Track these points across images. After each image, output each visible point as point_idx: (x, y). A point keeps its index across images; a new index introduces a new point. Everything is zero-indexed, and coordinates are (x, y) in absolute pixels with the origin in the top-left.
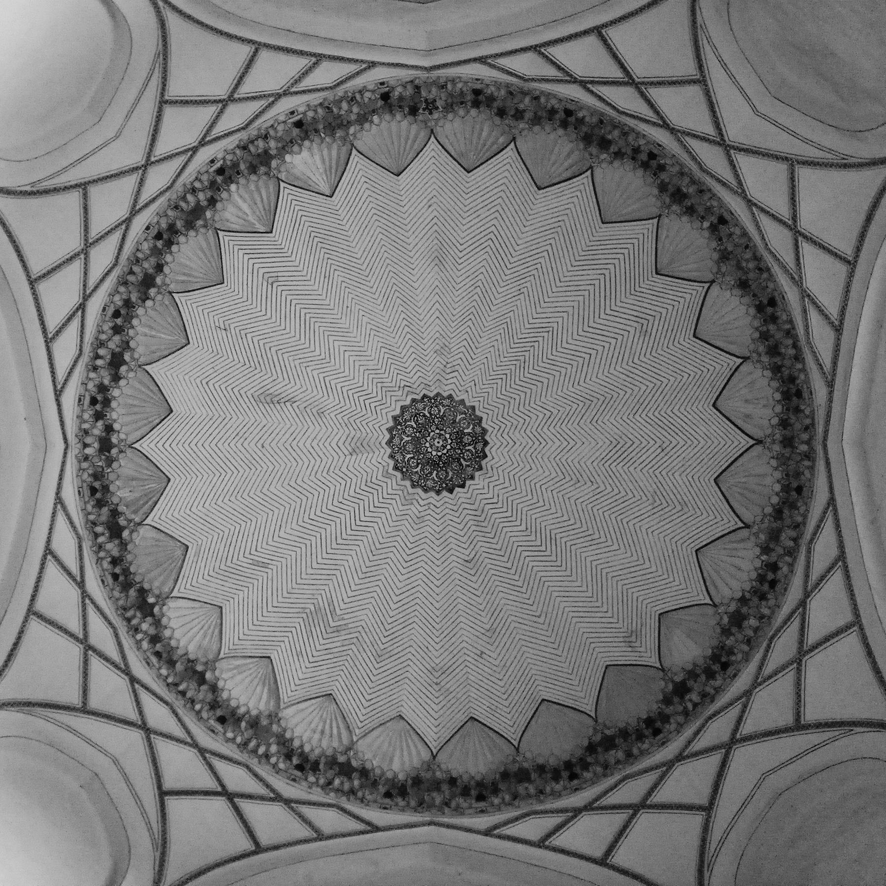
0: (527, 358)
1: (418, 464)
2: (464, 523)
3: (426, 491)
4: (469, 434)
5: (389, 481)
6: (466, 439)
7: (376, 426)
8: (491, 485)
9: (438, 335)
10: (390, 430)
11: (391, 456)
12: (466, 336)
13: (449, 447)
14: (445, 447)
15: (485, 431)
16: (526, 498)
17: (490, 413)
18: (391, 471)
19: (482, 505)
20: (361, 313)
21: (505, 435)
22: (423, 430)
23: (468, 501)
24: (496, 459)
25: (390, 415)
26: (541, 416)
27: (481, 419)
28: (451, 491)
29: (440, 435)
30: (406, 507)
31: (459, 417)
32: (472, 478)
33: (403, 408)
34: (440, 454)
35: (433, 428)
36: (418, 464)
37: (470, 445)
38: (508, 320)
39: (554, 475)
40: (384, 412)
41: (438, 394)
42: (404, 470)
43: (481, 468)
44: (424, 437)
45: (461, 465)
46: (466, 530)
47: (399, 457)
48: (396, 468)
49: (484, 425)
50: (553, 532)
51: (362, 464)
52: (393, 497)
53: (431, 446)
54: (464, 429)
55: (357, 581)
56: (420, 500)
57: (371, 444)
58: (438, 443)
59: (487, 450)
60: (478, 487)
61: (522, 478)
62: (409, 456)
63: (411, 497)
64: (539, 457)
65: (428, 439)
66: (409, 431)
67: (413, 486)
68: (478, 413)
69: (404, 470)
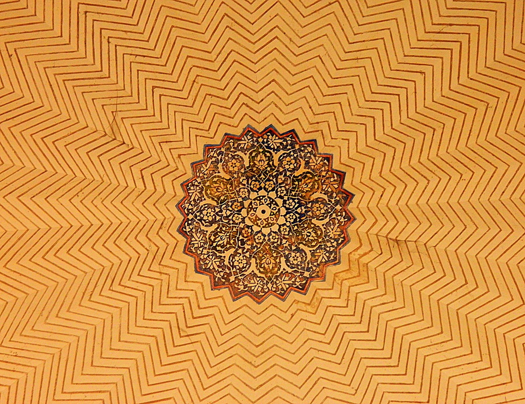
0: (129, 51)
1: (298, 250)
2: (406, 178)
3: (346, 240)
4: (252, 159)
5: (326, 302)
6: (262, 164)
7: (228, 318)
8: (342, 126)
9: (76, 201)
10: (236, 295)
11: (282, 295)
12: (82, 152)
13: (273, 195)
14: (272, 201)
15: (249, 131)
16: (369, 68)
17: (218, 119)
18: (306, 298)
19: (376, 145)
20: (28, 331)
21: (258, 97)
22: (240, 238)
23: (368, 168)
24: (298, 114)
25: (211, 293)
26: (229, 33)
27: (228, 136)
28: (348, 197)
29: (250, 208)
30: (372, 275)
31: (222, 174)
32: (328, 158)
33: (199, 270)
34: (283, 211)
35: (237, 219)
36: (298, 250)
37: (270, 159)
38: (60, 78)
39: (331, 19)
40: (203, 303)
41: (180, 207)
42: (307, 274)
43: (313, 143)
44: (252, 236)
45: (304, 176)
46: (417, 176)
47: (284, 283)
48: (303, 289)
49: (238, 132)
50: (429, 27)
51: (292, 348)
52: (352, 298)
53: (269, 225)
54: (243, 166)
55: (494, 371)
56: (361, 252)
57: (258, 330)
58: (263, 212)
59: (281, 129)
60: (344, 150)
61: (334, 73)
62: (283, 265)
63: (355, 267)
64: (300, 42)
65: (256, 229)
66: (240, 261)
67: (336, 261)
68: (217, 141)
69: (307, 274)
